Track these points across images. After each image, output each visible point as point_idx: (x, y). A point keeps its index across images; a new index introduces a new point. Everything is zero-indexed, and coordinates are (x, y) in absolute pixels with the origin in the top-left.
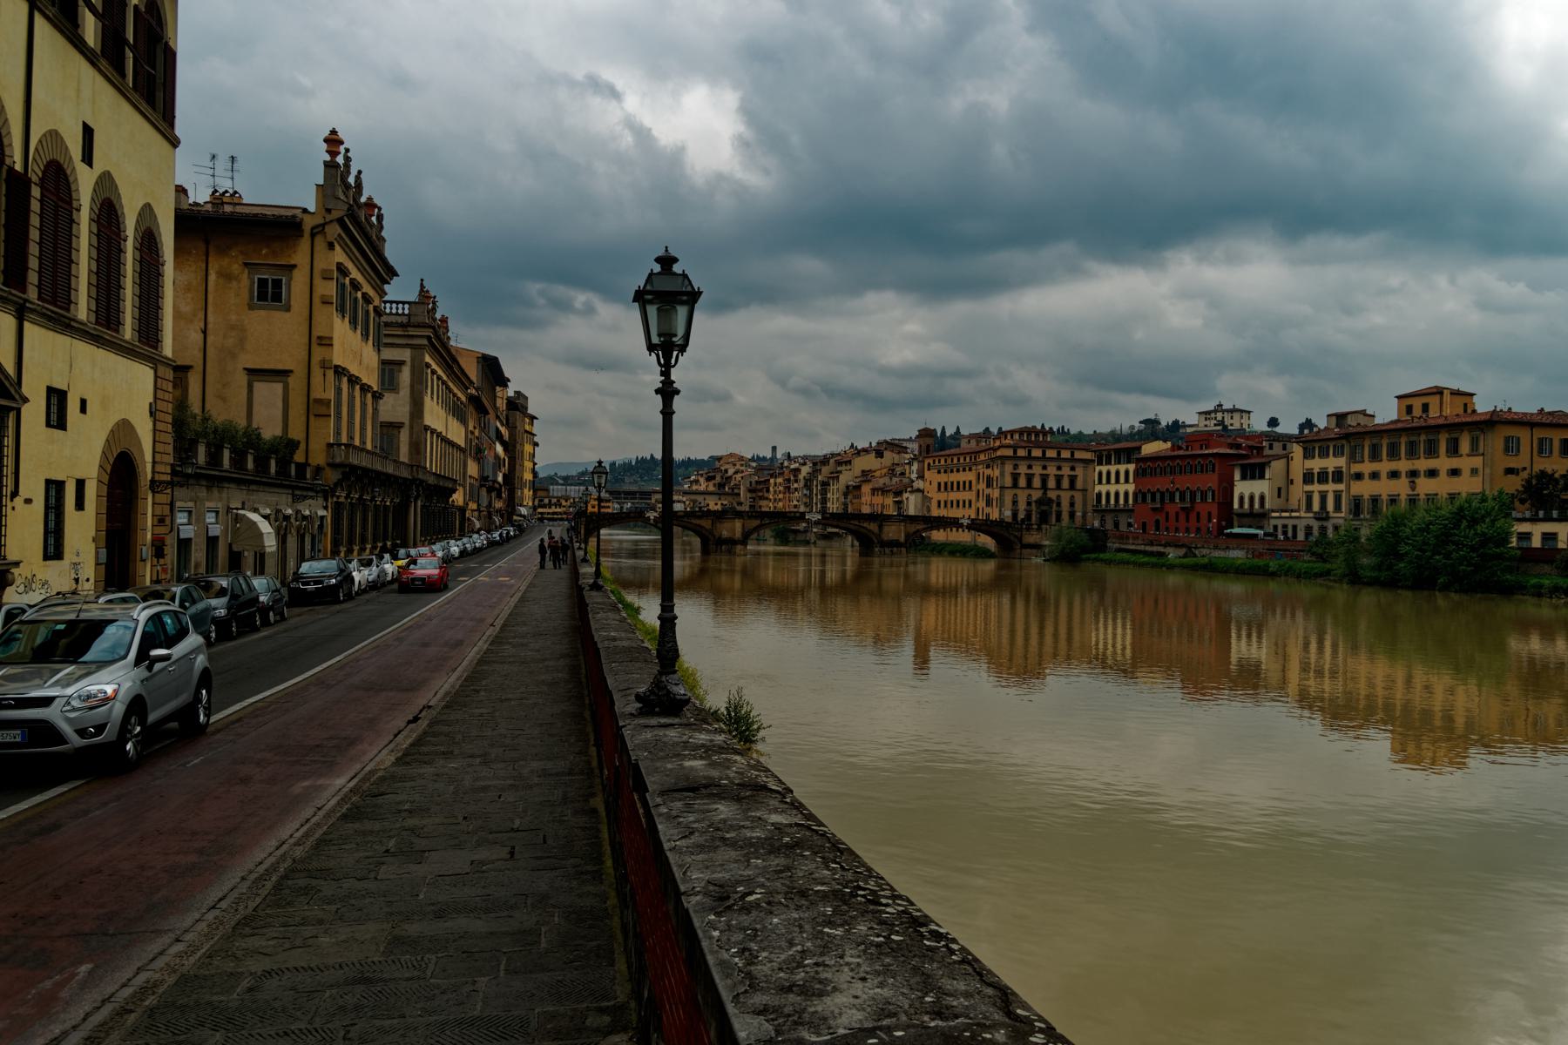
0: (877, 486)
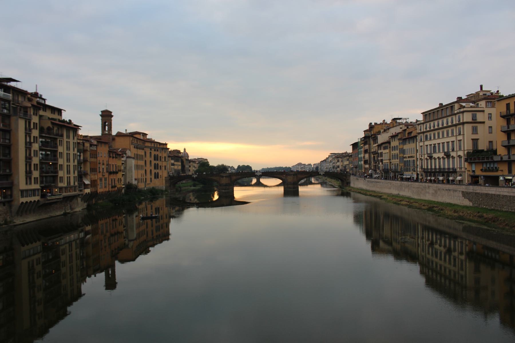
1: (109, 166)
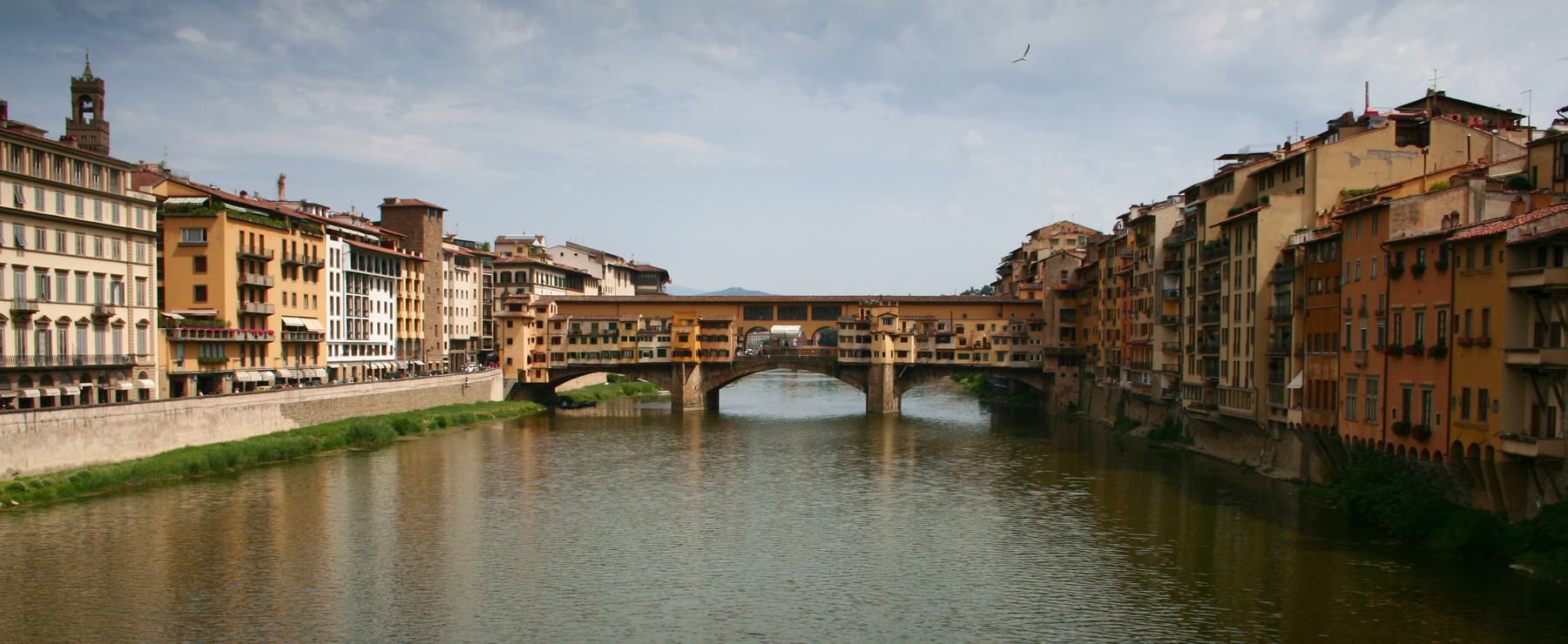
0: (1411, 232)
1: (1391, 319)
